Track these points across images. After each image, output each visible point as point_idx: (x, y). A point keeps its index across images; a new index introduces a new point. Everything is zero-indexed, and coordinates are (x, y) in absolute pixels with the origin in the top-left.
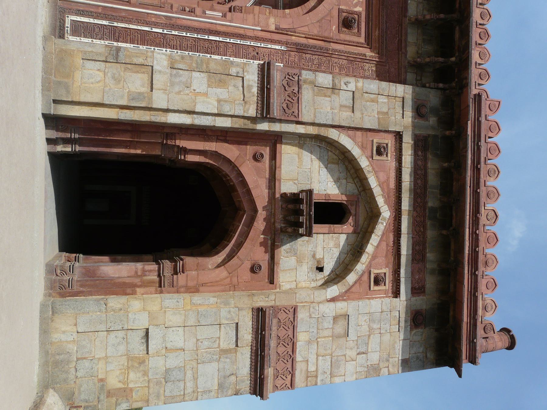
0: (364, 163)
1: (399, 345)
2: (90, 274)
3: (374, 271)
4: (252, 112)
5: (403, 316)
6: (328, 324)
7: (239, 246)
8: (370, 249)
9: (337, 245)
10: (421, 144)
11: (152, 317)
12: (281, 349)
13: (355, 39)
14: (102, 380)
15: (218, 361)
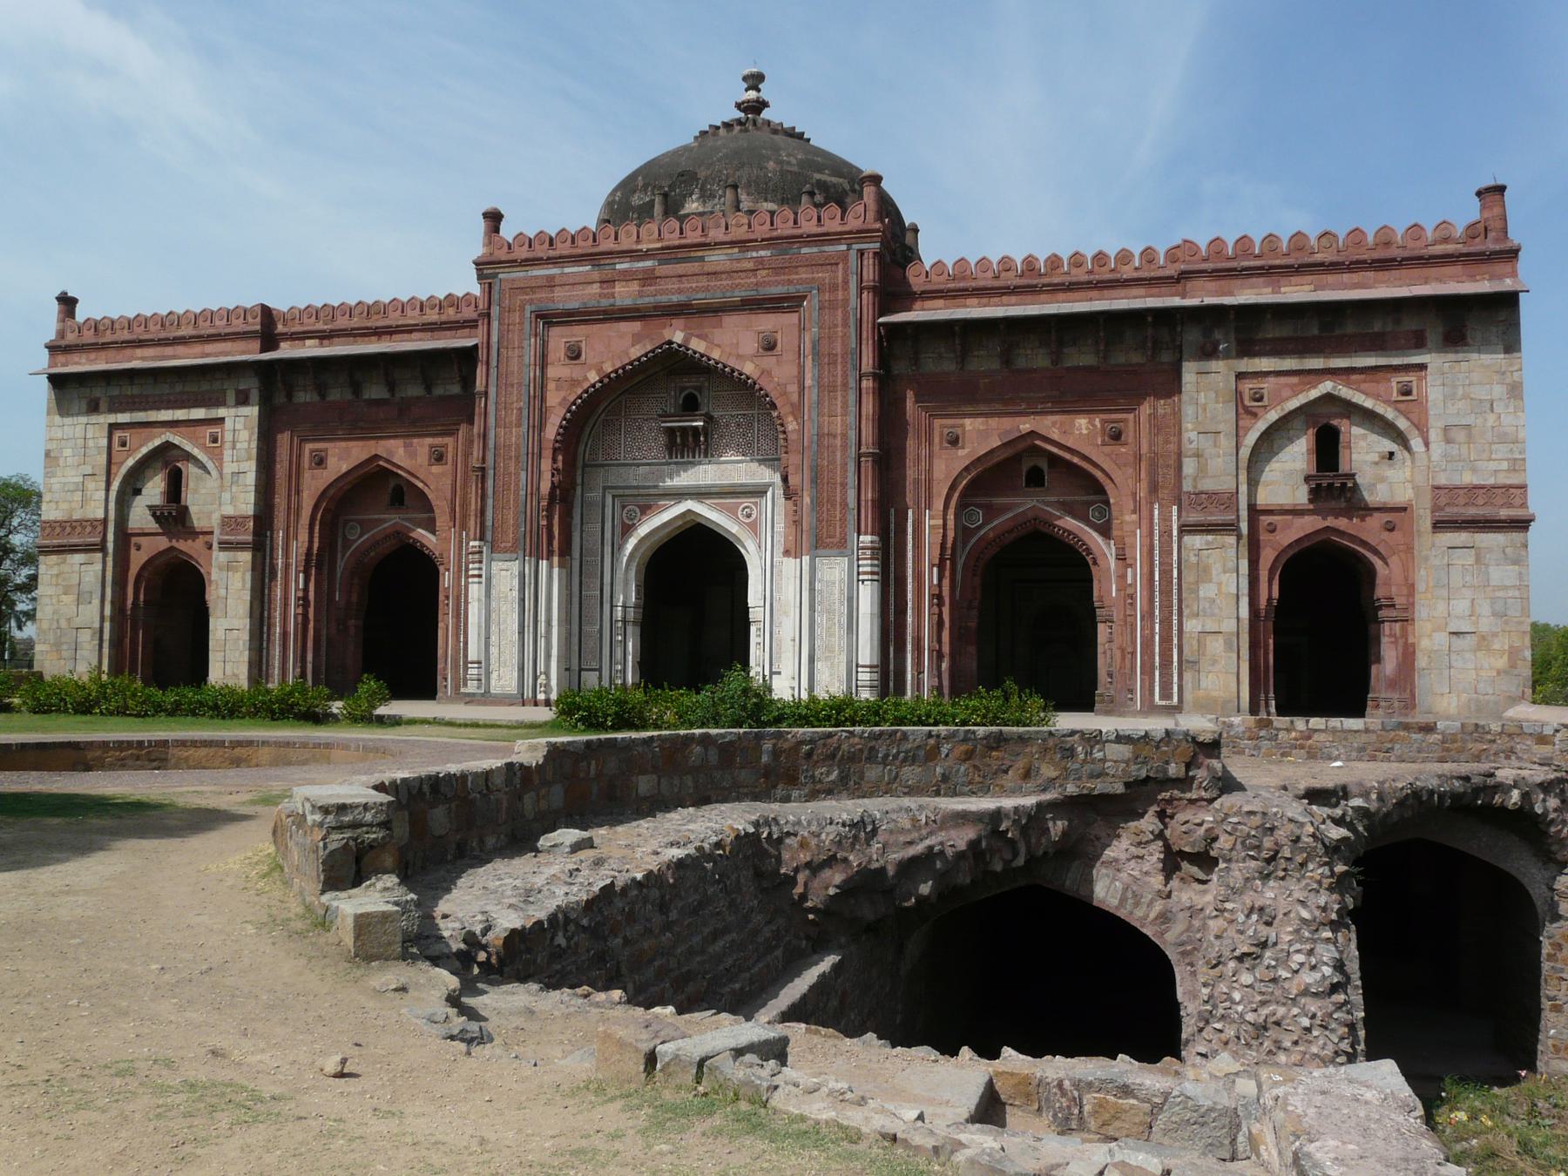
0: (1273, 416)
1: (1486, 358)
2: (1393, 684)
3: (1395, 396)
4: (1232, 540)
5: (1451, 356)
6: (1454, 450)
7: (1364, 544)
8: (1368, 403)
9: (1364, 437)
10: (1247, 348)
11: (1437, 629)
12: (1480, 501)
13: (1131, 424)
14: (1499, 673)
15: (1487, 566)
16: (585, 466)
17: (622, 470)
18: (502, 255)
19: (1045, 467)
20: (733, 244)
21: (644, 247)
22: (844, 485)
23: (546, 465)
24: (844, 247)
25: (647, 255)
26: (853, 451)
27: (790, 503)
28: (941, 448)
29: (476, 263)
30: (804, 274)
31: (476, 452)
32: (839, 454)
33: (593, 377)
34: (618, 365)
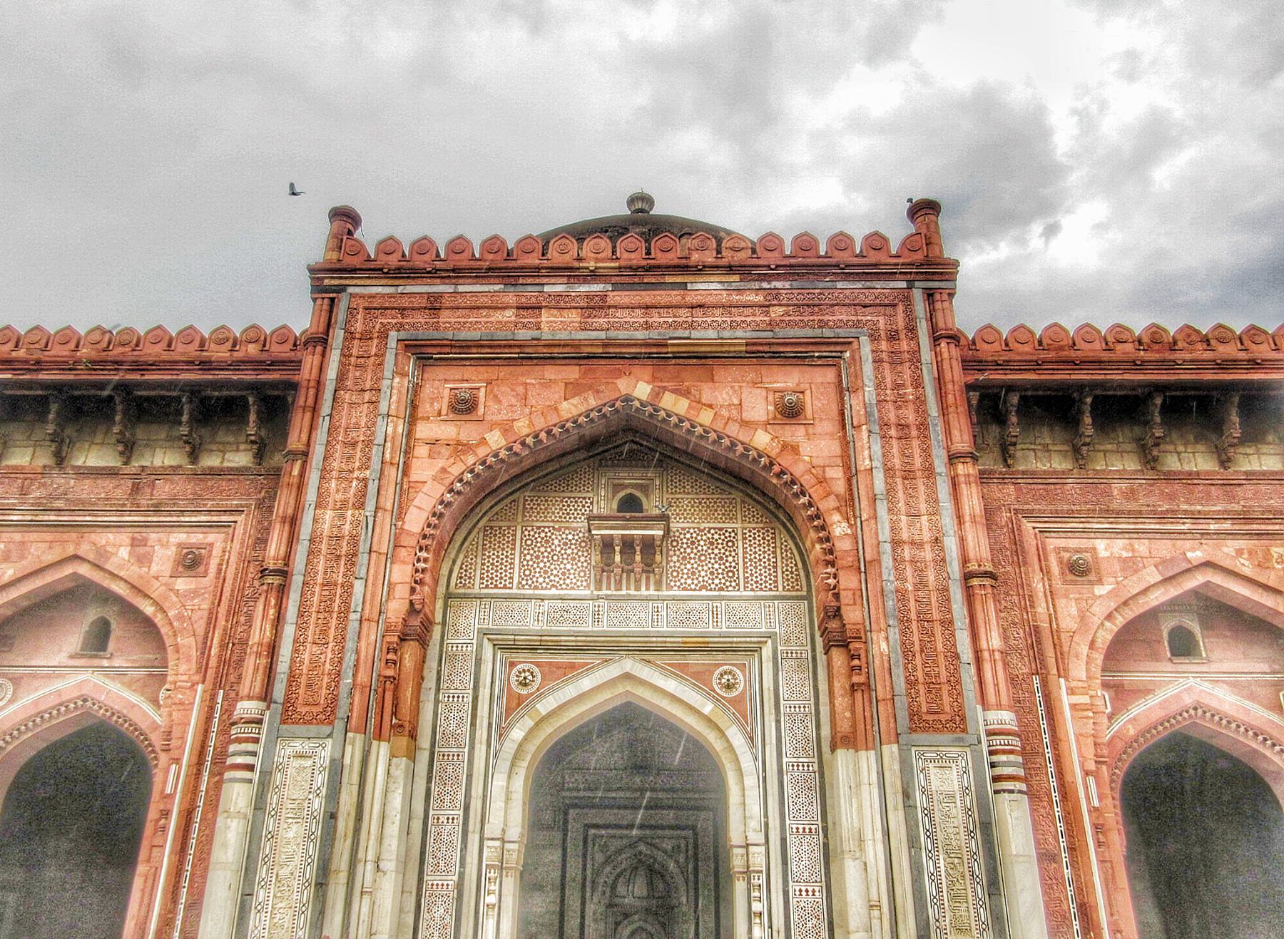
16: (448, 596)
17: (517, 604)
18: (356, 262)
19: (1196, 628)
20: (730, 269)
21: (592, 265)
22: (948, 624)
23: (401, 573)
24: (904, 285)
25: (594, 276)
26: (955, 569)
27: (838, 657)
28: (1065, 582)
29: (312, 270)
30: (842, 315)
31: (275, 548)
32: (931, 576)
33: (496, 440)
34: (540, 423)
